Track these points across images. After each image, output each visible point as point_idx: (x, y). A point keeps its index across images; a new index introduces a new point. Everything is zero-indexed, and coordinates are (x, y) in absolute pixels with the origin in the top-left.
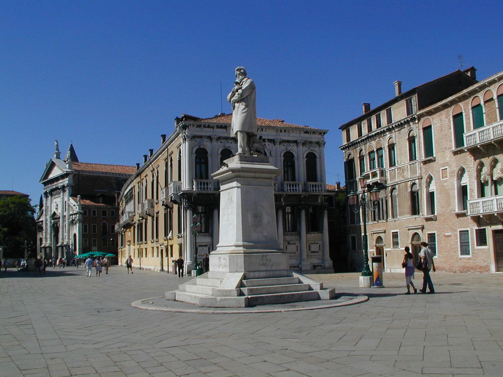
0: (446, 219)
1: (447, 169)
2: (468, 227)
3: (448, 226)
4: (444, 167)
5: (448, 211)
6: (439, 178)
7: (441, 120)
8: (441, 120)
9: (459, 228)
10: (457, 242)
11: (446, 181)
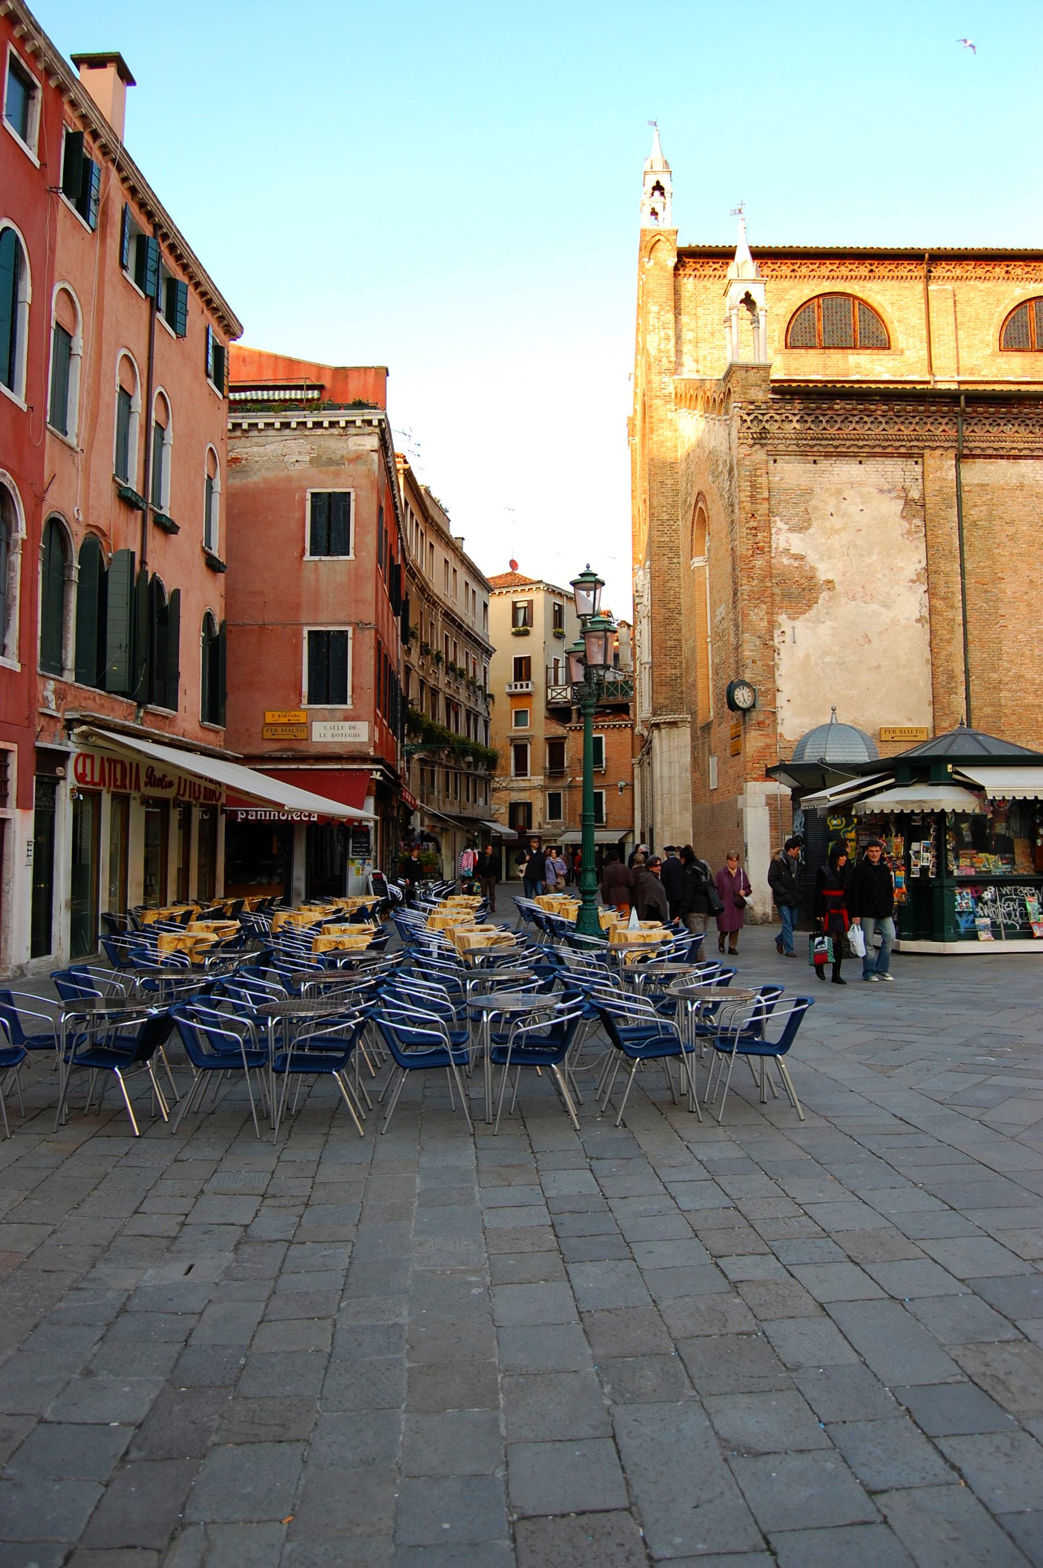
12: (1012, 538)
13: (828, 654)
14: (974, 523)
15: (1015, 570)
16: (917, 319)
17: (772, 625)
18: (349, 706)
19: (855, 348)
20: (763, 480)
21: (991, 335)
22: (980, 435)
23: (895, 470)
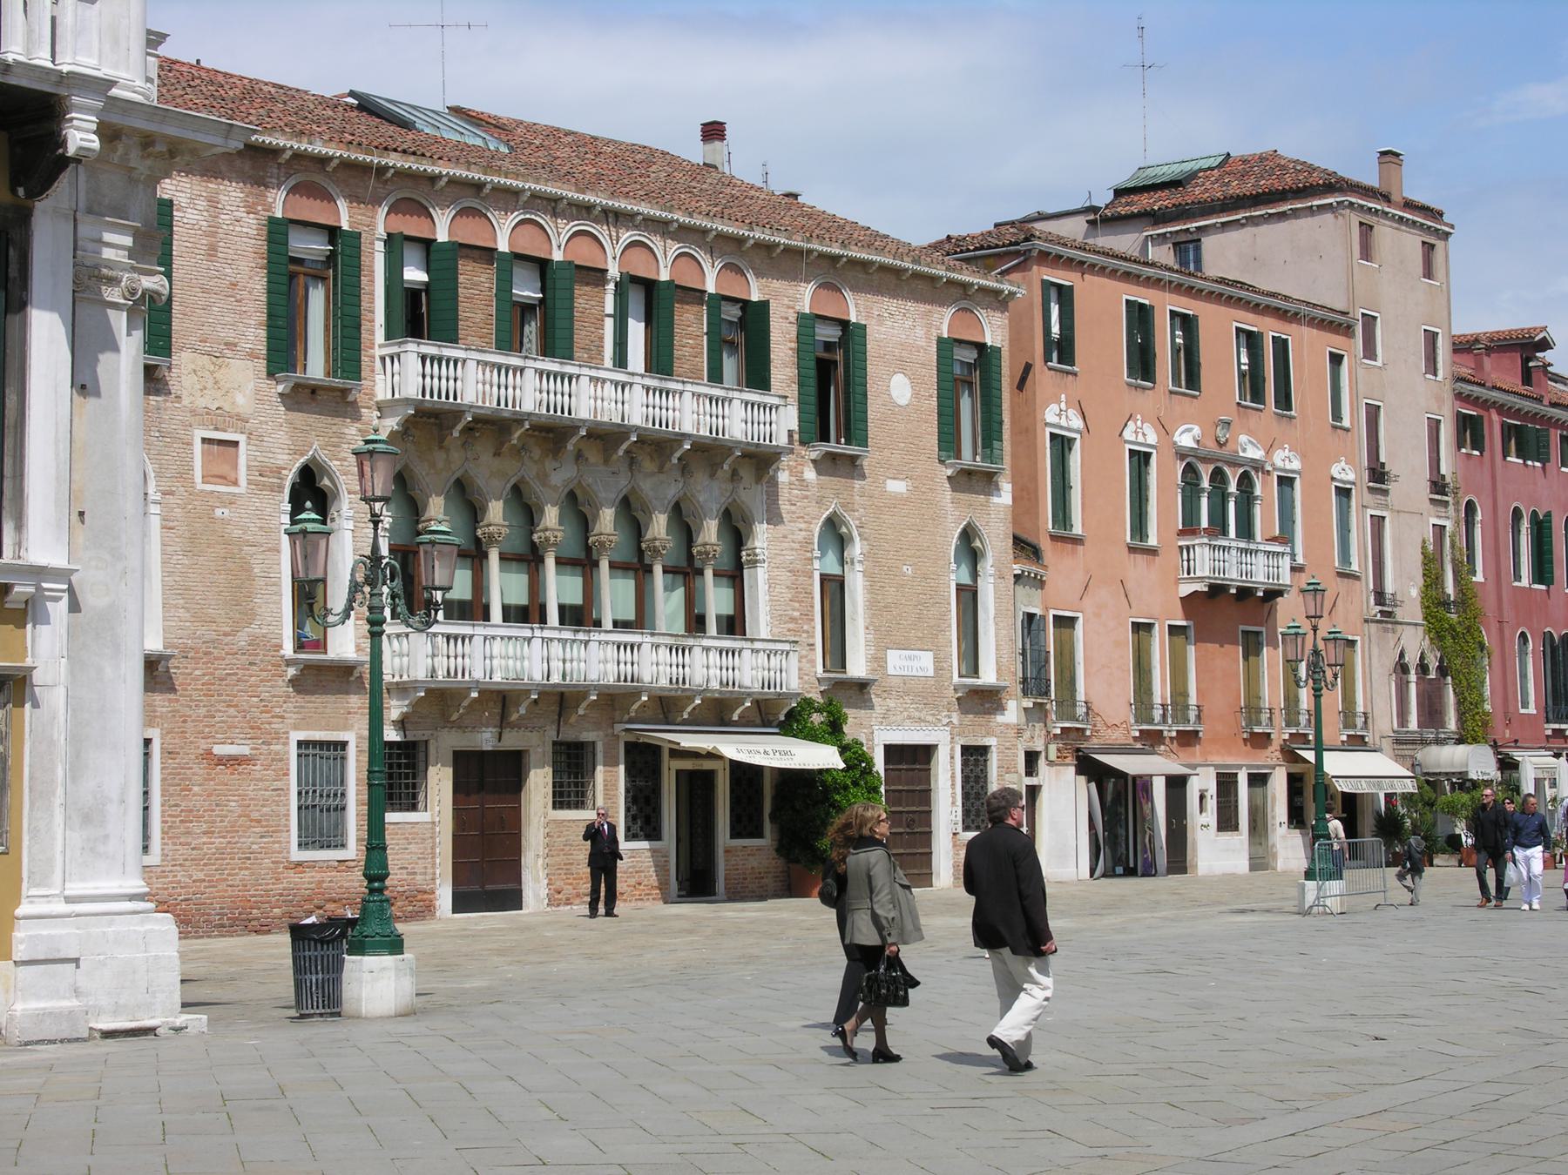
0: (221, 680)
1: (236, 444)
2: (346, 728)
3: (232, 711)
4: (216, 429)
5: (242, 640)
6: (184, 475)
7: (213, 202)
8: (213, 202)
9: (296, 728)
10: (283, 791)
11: (230, 501)
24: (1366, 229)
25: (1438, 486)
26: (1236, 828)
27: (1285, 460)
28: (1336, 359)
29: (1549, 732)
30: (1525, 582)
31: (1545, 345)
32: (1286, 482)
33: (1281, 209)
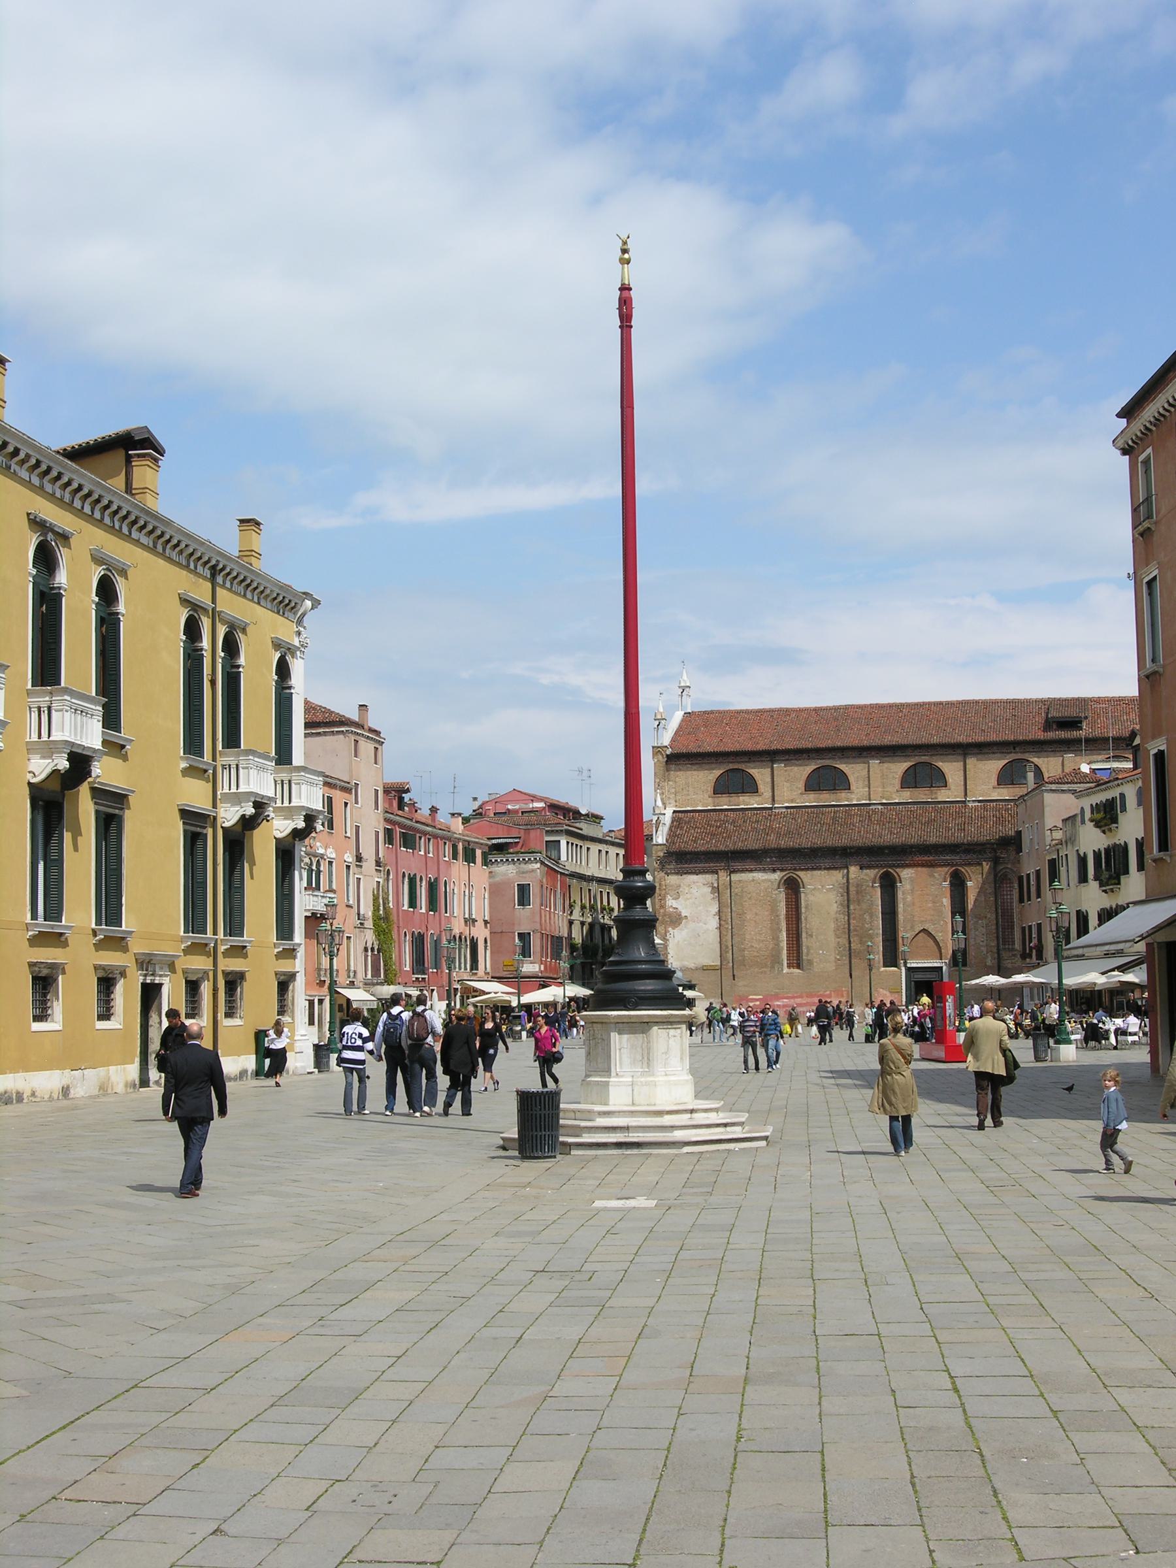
12: (750, 898)
13: (685, 941)
14: (736, 894)
15: (751, 910)
16: (769, 779)
17: (666, 932)
18: (532, 958)
19: (743, 793)
20: (663, 883)
21: (801, 785)
22: (738, 866)
23: (709, 878)
24: (356, 741)
25: (378, 863)
26: (313, 1024)
27: (331, 853)
28: (346, 804)
29: (414, 979)
30: (406, 907)
31: (408, 791)
32: (330, 863)
33: (318, 731)
